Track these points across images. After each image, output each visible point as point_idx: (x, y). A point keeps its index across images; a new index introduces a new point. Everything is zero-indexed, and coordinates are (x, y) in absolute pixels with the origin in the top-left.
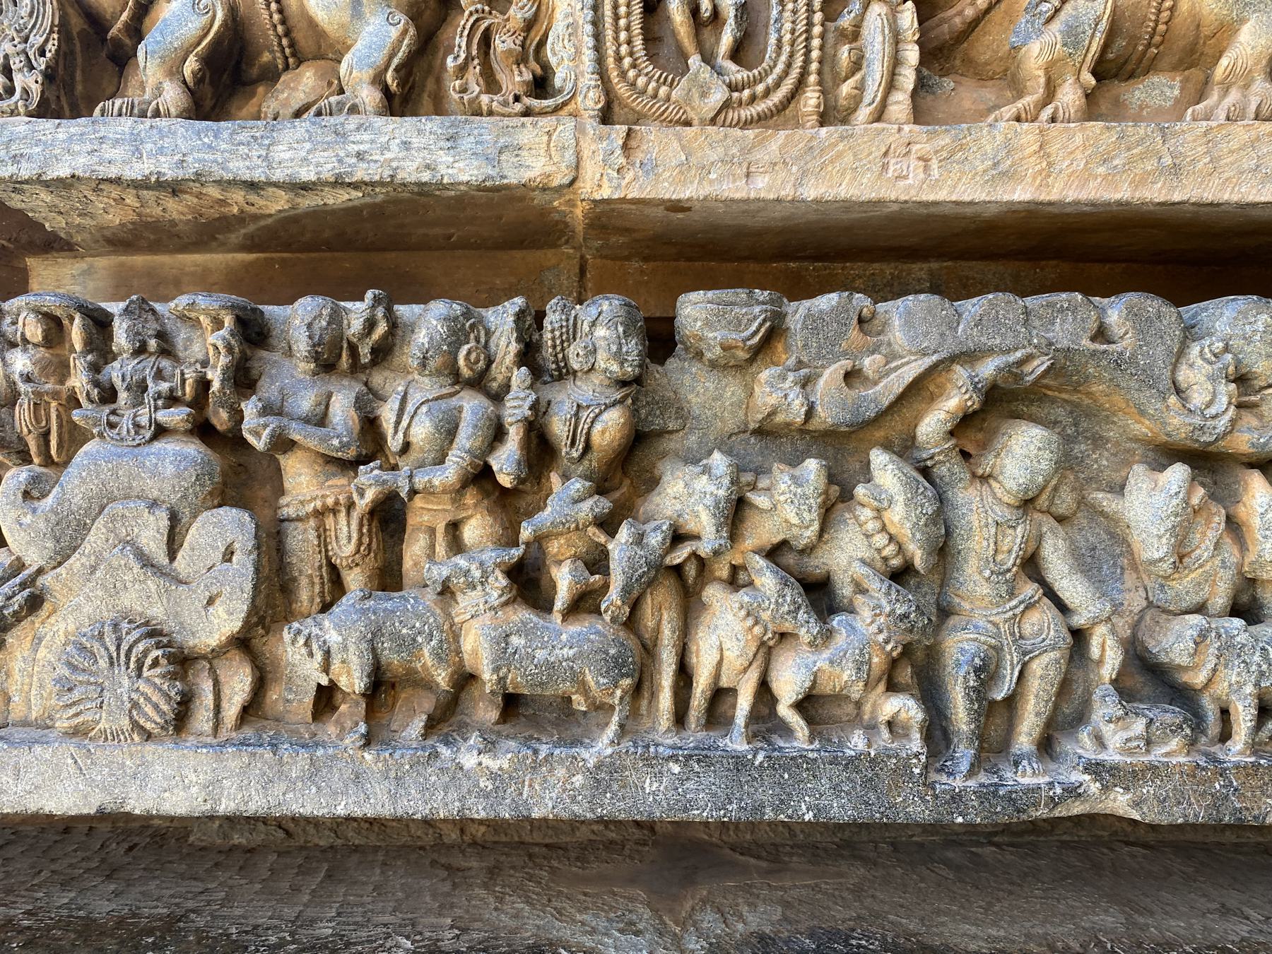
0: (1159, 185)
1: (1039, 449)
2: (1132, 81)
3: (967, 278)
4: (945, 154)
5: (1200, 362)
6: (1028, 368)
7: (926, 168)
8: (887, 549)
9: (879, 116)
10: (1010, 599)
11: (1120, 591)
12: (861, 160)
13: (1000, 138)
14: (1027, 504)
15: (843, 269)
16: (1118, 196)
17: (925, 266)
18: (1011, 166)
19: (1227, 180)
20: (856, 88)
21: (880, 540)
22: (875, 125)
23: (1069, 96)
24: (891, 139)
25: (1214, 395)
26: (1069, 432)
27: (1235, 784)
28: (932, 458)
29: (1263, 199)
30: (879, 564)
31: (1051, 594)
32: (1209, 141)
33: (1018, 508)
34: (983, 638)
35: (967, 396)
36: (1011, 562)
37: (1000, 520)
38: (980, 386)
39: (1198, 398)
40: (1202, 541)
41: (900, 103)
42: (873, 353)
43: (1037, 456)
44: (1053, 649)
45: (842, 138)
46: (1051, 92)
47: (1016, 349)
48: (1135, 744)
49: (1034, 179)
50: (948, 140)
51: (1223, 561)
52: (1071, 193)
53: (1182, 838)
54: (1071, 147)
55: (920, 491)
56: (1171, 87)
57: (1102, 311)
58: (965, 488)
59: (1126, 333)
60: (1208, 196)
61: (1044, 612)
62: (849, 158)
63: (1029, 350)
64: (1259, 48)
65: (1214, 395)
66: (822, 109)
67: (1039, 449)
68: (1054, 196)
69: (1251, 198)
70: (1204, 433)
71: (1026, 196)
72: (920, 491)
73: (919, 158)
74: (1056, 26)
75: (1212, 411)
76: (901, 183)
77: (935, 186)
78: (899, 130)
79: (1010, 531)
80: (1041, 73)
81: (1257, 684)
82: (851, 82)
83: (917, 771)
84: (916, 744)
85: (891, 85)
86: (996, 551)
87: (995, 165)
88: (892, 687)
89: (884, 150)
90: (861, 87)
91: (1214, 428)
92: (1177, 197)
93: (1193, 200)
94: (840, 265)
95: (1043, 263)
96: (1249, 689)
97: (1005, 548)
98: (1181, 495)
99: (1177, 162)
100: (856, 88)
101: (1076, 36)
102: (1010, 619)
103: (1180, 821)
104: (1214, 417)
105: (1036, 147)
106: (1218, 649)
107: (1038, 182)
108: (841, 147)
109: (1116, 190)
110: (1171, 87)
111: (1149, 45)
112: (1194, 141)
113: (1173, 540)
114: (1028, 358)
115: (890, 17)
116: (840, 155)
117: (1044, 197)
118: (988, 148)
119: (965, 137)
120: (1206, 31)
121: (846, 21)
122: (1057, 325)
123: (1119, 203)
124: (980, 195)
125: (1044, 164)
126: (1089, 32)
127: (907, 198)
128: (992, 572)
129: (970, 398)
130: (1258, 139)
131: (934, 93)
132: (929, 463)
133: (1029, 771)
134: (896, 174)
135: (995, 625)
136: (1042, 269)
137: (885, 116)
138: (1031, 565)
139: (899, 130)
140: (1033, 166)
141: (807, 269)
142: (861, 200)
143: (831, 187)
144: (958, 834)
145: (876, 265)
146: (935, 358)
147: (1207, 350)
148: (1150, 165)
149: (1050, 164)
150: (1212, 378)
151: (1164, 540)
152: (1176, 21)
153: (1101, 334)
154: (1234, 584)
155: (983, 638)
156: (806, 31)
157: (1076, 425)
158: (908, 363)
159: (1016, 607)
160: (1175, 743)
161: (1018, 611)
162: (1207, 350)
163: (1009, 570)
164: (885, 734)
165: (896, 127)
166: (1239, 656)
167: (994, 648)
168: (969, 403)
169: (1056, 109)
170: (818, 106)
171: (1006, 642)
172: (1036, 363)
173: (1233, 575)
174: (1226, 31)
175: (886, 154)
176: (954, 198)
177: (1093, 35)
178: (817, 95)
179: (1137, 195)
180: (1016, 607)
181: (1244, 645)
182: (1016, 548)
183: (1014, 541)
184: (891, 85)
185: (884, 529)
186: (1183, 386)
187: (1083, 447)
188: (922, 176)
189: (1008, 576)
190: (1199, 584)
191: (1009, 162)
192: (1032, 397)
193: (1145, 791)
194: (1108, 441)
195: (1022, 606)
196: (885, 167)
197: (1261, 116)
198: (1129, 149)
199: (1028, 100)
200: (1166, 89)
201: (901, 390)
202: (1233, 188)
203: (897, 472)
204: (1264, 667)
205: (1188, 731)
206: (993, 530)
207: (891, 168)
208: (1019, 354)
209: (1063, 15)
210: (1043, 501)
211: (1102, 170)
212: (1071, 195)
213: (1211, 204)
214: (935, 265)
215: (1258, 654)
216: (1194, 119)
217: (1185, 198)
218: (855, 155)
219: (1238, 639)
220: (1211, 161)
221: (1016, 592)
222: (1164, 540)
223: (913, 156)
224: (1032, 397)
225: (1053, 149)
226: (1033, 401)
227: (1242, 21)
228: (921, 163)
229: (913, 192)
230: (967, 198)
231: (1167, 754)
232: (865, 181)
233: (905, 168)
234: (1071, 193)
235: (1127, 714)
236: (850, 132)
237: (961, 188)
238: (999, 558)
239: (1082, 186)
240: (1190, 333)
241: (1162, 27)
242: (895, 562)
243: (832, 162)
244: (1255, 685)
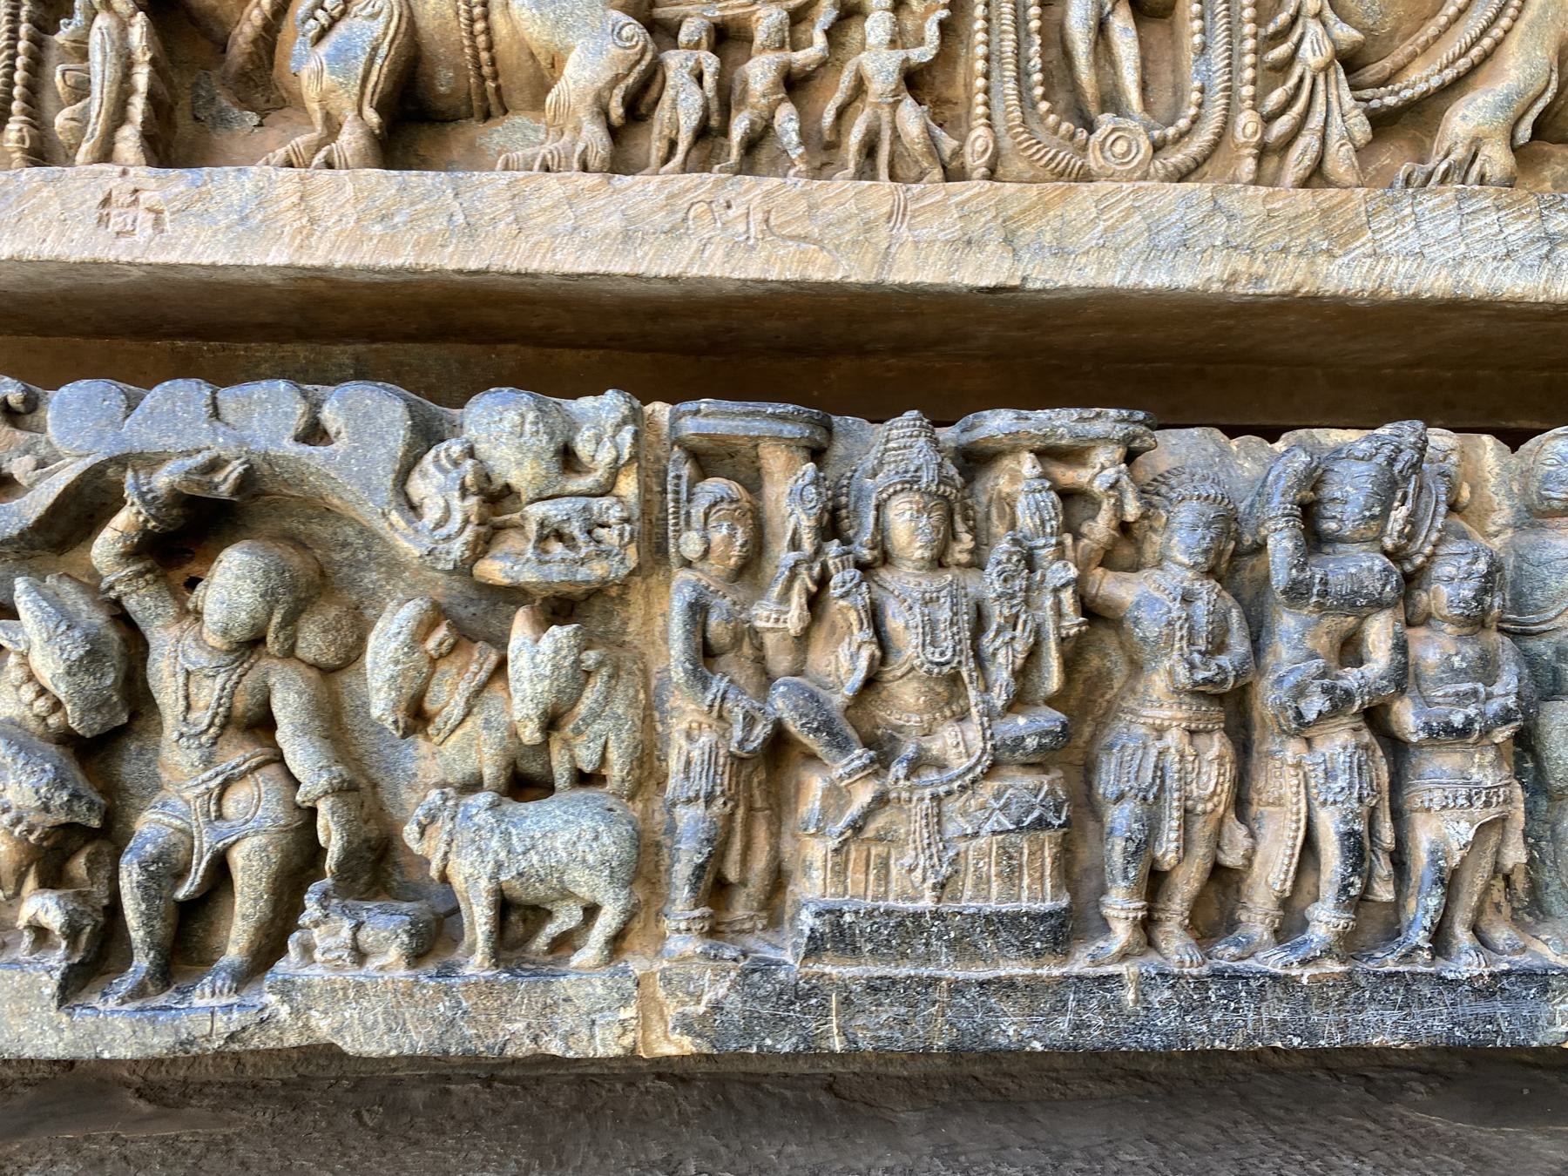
0: (451, 249)
1: (238, 578)
2: (490, 122)
3: (401, 364)
4: (178, 205)
5: (432, 469)
6: (218, 478)
7: (158, 223)
8: (37, 704)
9: (106, 153)
10: (205, 770)
11: (413, 759)
12: (71, 209)
13: (249, 185)
14: (250, 645)
15: (246, 350)
16: (396, 262)
17: (350, 349)
18: (262, 221)
19: (536, 244)
20: (73, 119)
21: (28, 693)
22: (97, 167)
23: (350, 139)
24: (112, 184)
25: (448, 510)
26: (361, 556)
27: (464, 1004)
28: (111, 588)
29: (582, 269)
30: (33, 724)
31: (279, 759)
32: (514, 196)
33: (229, 652)
34: (166, 820)
35: (134, 510)
36: (206, 721)
37: (191, 668)
38: (149, 496)
39: (432, 514)
40: (451, 693)
41: (129, 141)
42: (27, 452)
43: (235, 586)
44: (257, 833)
45: (46, 182)
46: (332, 127)
47: (199, 451)
48: (336, 954)
49: (293, 238)
50: (182, 188)
51: (487, 721)
52: (339, 257)
53: (743, 1068)
54: (342, 199)
55: (60, 631)
56: (536, 131)
57: (315, 407)
58: (165, 627)
59: (338, 433)
60: (513, 265)
61: (257, 785)
62: (55, 207)
63: (213, 453)
64: (582, 82)
65: (448, 510)
66: (27, 145)
67: (238, 578)
68: (318, 261)
69: (569, 267)
70: (438, 559)
71: (282, 260)
72: (60, 631)
73: (149, 210)
74: (325, 47)
75: (444, 531)
76: (123, 241)
77: (165, 247)
78: (124, 173)
79: (208, 682)
80: (315, 106)
81: (494, 877)
82: (67, 112)
83: (47, 991)
84: (57, 959)
85: (119, 116)
86: (188, 708)
87: (244, 219)
88: (53, 878)
89: (101, 197)
90: (82, 120)
91: (448, 553)
92: (473, 265)
93: (494, 268)
94: (242, 345)
95: (500, 347)
96: (484, 883)
97: (201, 704)
98: (401, 637)
99: (472, 220)
100: (73, 119)
101: (346, 61)
102: (203, 794)
103: (393, 1053)
104: (448, 538)
105: (295, 199)
106: (450, 833)
107: (297, 241)
108: (45, 193)
109: (397, 255)
110: (536, 131)
111: (482, 78)
112: (496, 195)
113: (393, 694)
114: (215, 465)
115: (115, 33)
116: (44, 204)
117: (305, 261)
118: (235, 198)
119: (205, 184)
120: (544, 62)
121: (63, 36)
122: (255, 423)
123: (399, 270)
124: (223, 259)
125: (305, 220)
126: (363, 58)
127: (129, 259)
128: (182, 735)
129: (139, 513)
130: (577, 195)
131: (231, 129)
132: (112, 595)
133: (208, 991)
134: (117, 229)
135: (187, 802)
136: (498, 355)
137: (115, 155)
138: (261, 724)
139: (124, 173)
140: (292, 221)
141: (200, 350)
142: (72, 260)
143: (33, 243)
144: (453, 1067)
145: (288, 347)
146: (88, 462)
147: (443, 455)
148: (439, 224)
149: (312, 221)
150: (442, 490)
151: (382, 695)
152: (499, 48)
153: (314, 433)
154: (505, 749)
155: (166, 820)
156: (9, 47)
157: (368, 547)
158: (64, 466)
159: (210, 779)
160: (394, 953)
161: (212, 784)
162: (443, 455)
163: (206, 731)
164: (27, 939)
165: (119, 169)
166: (473, 841)
167: (182, 831)
168: (141, 519)
169: (330, 152)
170: (22, 140)
171: (195, 824)
172: (230, 468)
173: (503, 738)
174: (556, 63)
175: (106, 202)
176: (189, 260)
177: (371, 61)
178: (17, 126)
179: (422, 261)
180: (210, 779)
181: (480, 828)
182: (214, 704)
183: (208, 694)
184: (119, 116)
185: (31, 677)
186: (416, 499)
187: (374, 576)
188: (150, 231)
189: (204, 739)
190: (462, 749)
191: (260, 217)
192: (310, 511)
193: (347, 1015)
194: (406, 568)
195: (220, 779)
196: (103, 221)
197: (591, 168)
198: (412, 204)
199: (301, 140)
200: (529, 132)
201: (51, 501)
202: (545, 255)
203: (29, 605)
204: (503, 855)
205: (405, 938)
206: (181, 679)
207: (112, 221)
208: (201, 459)
209: (333, 37)
210: (272, 645)
211: (378, 228)
212: (339, 260)
213: (518, 274)
214: (361, 348)
215: (496, 838)
216: (506, 168)
217: (483, 266)
218: (63, 204)
219: (476, 819)
220: (516, 220)
221: (217, 759)
222: (382, 695)
223: (142, 207)
224: (310, 511)
225: (318, 202)
226: (310, 517)
227: (569, 49)
228: (152, 216)
229: (137, 252)
230: (205, 261)
231: (382, 968)
232: (76, 236)
233: (129, 221)
234: (339, 257)
235: (326, 916)
236: (57, 175)
237: (199, 248)
238: (192, 716)
239: (352, 250)
240: (426, 435)
241: (484, 56)
242: (53, 721)
243: (33, 212)
244: (491, 878)
